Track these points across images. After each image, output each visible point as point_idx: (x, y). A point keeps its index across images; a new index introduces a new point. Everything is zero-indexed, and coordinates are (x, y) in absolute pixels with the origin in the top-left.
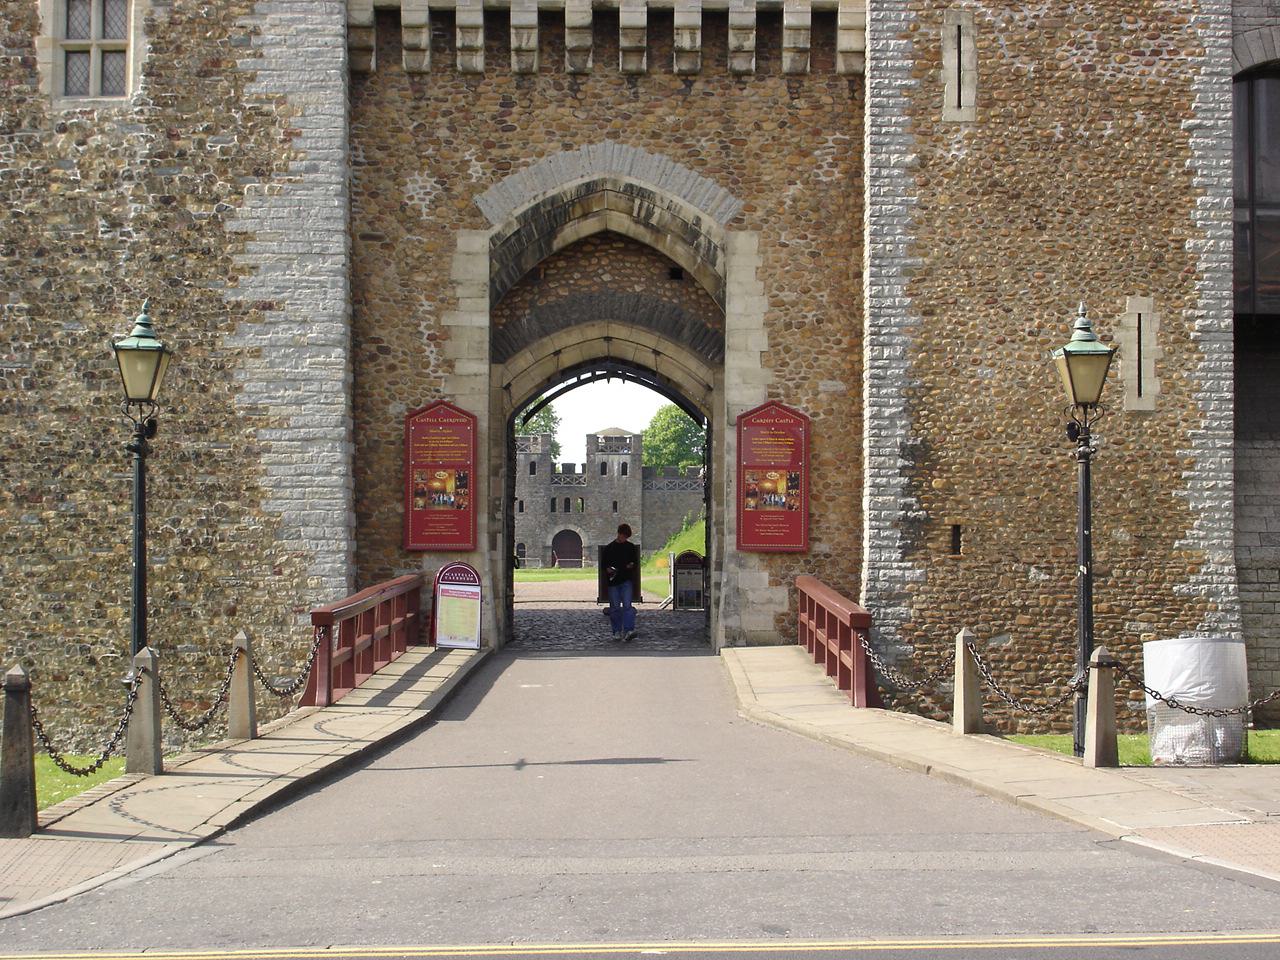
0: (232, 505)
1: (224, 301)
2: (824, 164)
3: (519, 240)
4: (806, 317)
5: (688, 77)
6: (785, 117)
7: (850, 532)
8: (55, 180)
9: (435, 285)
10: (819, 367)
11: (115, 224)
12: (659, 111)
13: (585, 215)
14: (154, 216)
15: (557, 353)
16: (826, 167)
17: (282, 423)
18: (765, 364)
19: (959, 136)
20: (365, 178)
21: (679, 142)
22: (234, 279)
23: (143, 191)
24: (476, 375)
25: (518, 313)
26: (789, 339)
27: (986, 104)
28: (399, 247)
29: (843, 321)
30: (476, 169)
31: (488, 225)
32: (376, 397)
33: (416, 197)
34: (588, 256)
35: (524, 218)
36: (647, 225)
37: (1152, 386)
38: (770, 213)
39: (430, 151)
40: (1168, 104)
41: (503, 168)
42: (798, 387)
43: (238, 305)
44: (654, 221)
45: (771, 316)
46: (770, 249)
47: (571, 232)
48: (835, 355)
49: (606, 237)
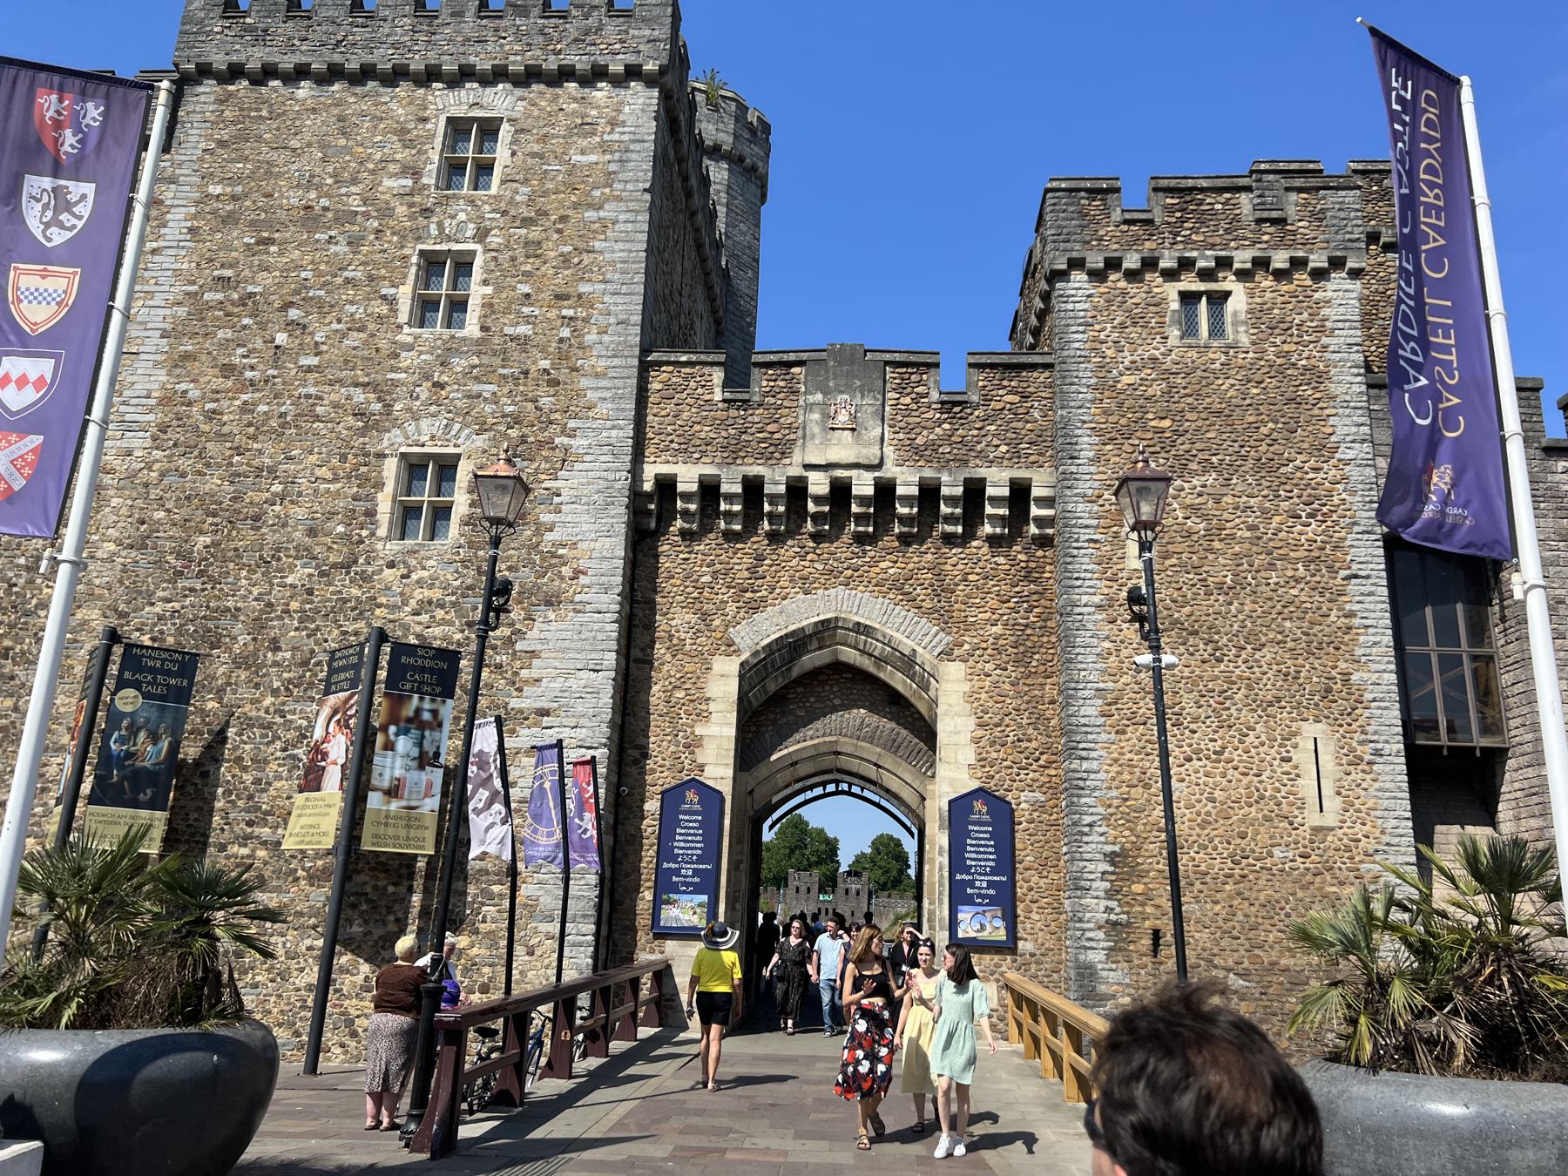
1: (510, 707)
8: (380, 606)
12: (883, 565)
13: (820, 648)
21: (900, 588)
22: (520, 690)
25: (763, 729)
30: (731, 608)
31: (737, 652)
37: (1332, 803)
40: (1324, 559)
41: (754, 607)
43: (521, 711)
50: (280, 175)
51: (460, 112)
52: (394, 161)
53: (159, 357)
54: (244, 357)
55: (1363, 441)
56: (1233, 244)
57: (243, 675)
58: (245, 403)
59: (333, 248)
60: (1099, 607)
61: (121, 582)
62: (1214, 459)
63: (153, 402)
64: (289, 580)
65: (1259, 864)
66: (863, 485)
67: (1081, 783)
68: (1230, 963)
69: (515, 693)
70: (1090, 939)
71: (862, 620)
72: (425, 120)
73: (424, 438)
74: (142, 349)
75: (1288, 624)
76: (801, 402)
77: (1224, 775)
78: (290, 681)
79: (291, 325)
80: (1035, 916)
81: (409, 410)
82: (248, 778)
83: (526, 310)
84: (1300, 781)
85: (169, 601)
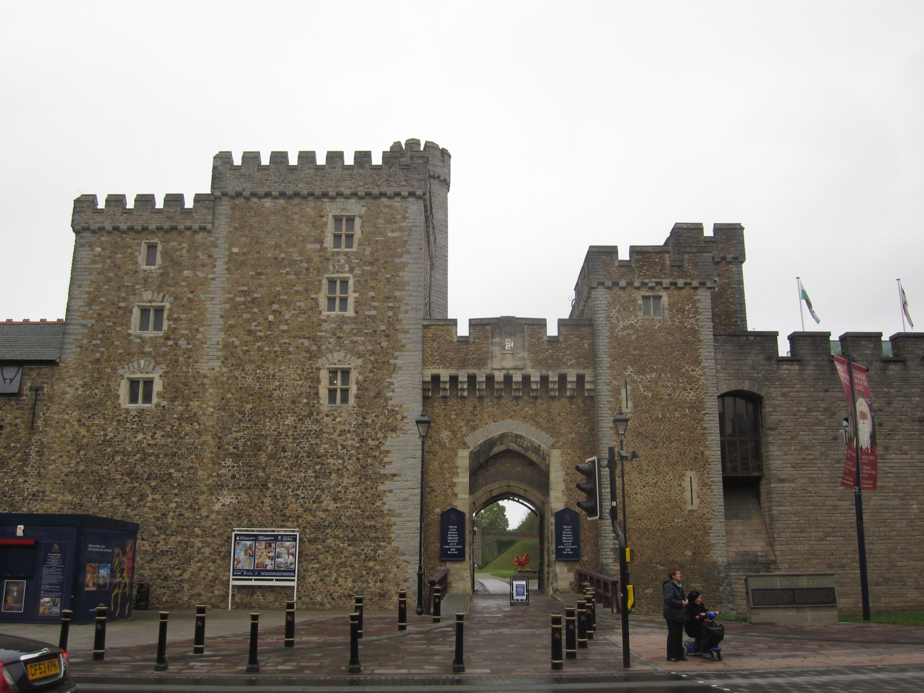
0: (382, 544)
5: (535, 398)
8: (324, 432)
11: (344, 447)
12: (526, 409)
13: (501, 444)
14: (358, 445)
15: (491, 491)
17: (399, 515)
21: (533, 419)
22: (384, 466)
23: (354, 436)
27: (635, 406)
28: (439, 455)
30: (464, 429)
31: (468, 448)
35: (481, 445)
36: (522, 447)
37: (696, 501)
38: (564, 443)
41: (474, 428)
43: (385, 475)
47: (497, 449)
50: (262, 243)
51: (338, 213)
52: (311, 236)
53: (220, 327)
54: (256, 326)
55: (711, 359)
56: (663, 276)
57: (273, 462)
58: (259, 346)
59: (289, 277)
61: (217, 424)
62: (655, 367)
63: (220, 347)
64: (286, 423)
66: (517, 378)
68: (658, 561)
71: (518, 433)
72: (322, 216)
73: (336, 361)
74: (212, 323)
75: (682, 433)
76: (490, 341)
77: (657, 492)
78: (292, 464)
79: (274, 312)
80: (588, 548)
81: (328, 348)
82: (280, 503)
83: (374, 304)
85: (238, 432)
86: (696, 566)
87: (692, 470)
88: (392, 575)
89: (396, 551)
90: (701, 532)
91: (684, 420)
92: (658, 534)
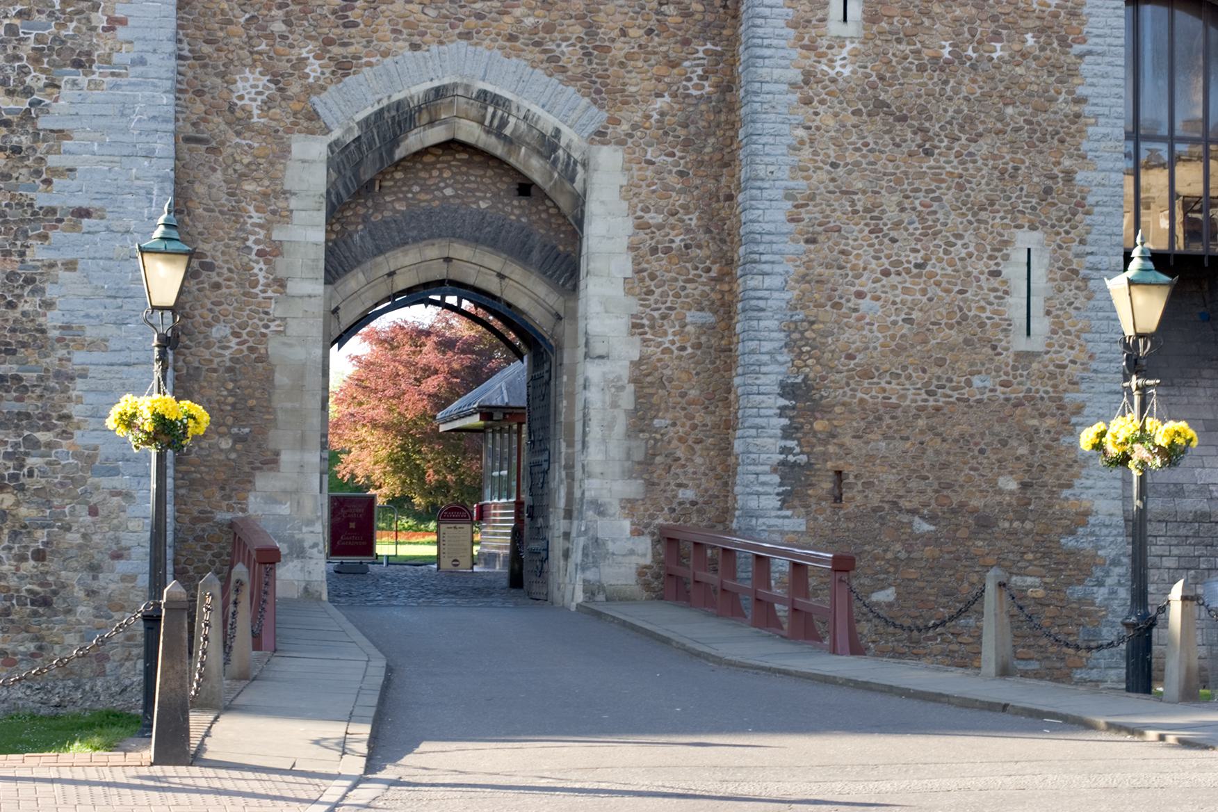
0: (42, 436)
1: (37, 206)
2: (694, 76)
3: (359, 148)
4: (673, 241)
6: (653, 23)
7: (718, 477)
9: (265, 195)
10: (687, 296)
12: (518, 12)
13: (432, 123)
15: (391, 274)
16: (695, 80)
17: (99, 344)
18: (629, 292)
19: (845, 53)
20: (190, 74)
22: (48, 182)
24: (310, 296)
25: (351, 228)
26: (656, 264)
29: (713, 246)
30: (314, 68)
31: (327, 130)
32: (198, 318)
33: (247, 97)
34: (429, 167)
36: (499, 135)
38: (635, 127)
39: (263, 47)
41: (344, 68)
42: (664, 317)
43: (53, 211)
44: (508, 131)
45: (636, 239)
46: (635, 167)
47: (415, 140)
48: (704, 284)
49: (452, 146)
60: (793, 85)
65: (956, 395)
67: (762, 304)
68: (915, 504)
69: (42, 187)
70: (763, 484)
71: (489, 88)
75: (1010, 110)
77: (924, 292)
80: (698, 460)
84: (1009, 300)
86: (1028, 525)
87: (1033, 228)
88: (74, 538)
89: (88, 458)
90: (1049, 422)
91: (1019, 70)
92: (921, 423)
